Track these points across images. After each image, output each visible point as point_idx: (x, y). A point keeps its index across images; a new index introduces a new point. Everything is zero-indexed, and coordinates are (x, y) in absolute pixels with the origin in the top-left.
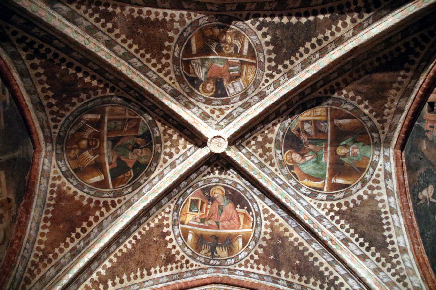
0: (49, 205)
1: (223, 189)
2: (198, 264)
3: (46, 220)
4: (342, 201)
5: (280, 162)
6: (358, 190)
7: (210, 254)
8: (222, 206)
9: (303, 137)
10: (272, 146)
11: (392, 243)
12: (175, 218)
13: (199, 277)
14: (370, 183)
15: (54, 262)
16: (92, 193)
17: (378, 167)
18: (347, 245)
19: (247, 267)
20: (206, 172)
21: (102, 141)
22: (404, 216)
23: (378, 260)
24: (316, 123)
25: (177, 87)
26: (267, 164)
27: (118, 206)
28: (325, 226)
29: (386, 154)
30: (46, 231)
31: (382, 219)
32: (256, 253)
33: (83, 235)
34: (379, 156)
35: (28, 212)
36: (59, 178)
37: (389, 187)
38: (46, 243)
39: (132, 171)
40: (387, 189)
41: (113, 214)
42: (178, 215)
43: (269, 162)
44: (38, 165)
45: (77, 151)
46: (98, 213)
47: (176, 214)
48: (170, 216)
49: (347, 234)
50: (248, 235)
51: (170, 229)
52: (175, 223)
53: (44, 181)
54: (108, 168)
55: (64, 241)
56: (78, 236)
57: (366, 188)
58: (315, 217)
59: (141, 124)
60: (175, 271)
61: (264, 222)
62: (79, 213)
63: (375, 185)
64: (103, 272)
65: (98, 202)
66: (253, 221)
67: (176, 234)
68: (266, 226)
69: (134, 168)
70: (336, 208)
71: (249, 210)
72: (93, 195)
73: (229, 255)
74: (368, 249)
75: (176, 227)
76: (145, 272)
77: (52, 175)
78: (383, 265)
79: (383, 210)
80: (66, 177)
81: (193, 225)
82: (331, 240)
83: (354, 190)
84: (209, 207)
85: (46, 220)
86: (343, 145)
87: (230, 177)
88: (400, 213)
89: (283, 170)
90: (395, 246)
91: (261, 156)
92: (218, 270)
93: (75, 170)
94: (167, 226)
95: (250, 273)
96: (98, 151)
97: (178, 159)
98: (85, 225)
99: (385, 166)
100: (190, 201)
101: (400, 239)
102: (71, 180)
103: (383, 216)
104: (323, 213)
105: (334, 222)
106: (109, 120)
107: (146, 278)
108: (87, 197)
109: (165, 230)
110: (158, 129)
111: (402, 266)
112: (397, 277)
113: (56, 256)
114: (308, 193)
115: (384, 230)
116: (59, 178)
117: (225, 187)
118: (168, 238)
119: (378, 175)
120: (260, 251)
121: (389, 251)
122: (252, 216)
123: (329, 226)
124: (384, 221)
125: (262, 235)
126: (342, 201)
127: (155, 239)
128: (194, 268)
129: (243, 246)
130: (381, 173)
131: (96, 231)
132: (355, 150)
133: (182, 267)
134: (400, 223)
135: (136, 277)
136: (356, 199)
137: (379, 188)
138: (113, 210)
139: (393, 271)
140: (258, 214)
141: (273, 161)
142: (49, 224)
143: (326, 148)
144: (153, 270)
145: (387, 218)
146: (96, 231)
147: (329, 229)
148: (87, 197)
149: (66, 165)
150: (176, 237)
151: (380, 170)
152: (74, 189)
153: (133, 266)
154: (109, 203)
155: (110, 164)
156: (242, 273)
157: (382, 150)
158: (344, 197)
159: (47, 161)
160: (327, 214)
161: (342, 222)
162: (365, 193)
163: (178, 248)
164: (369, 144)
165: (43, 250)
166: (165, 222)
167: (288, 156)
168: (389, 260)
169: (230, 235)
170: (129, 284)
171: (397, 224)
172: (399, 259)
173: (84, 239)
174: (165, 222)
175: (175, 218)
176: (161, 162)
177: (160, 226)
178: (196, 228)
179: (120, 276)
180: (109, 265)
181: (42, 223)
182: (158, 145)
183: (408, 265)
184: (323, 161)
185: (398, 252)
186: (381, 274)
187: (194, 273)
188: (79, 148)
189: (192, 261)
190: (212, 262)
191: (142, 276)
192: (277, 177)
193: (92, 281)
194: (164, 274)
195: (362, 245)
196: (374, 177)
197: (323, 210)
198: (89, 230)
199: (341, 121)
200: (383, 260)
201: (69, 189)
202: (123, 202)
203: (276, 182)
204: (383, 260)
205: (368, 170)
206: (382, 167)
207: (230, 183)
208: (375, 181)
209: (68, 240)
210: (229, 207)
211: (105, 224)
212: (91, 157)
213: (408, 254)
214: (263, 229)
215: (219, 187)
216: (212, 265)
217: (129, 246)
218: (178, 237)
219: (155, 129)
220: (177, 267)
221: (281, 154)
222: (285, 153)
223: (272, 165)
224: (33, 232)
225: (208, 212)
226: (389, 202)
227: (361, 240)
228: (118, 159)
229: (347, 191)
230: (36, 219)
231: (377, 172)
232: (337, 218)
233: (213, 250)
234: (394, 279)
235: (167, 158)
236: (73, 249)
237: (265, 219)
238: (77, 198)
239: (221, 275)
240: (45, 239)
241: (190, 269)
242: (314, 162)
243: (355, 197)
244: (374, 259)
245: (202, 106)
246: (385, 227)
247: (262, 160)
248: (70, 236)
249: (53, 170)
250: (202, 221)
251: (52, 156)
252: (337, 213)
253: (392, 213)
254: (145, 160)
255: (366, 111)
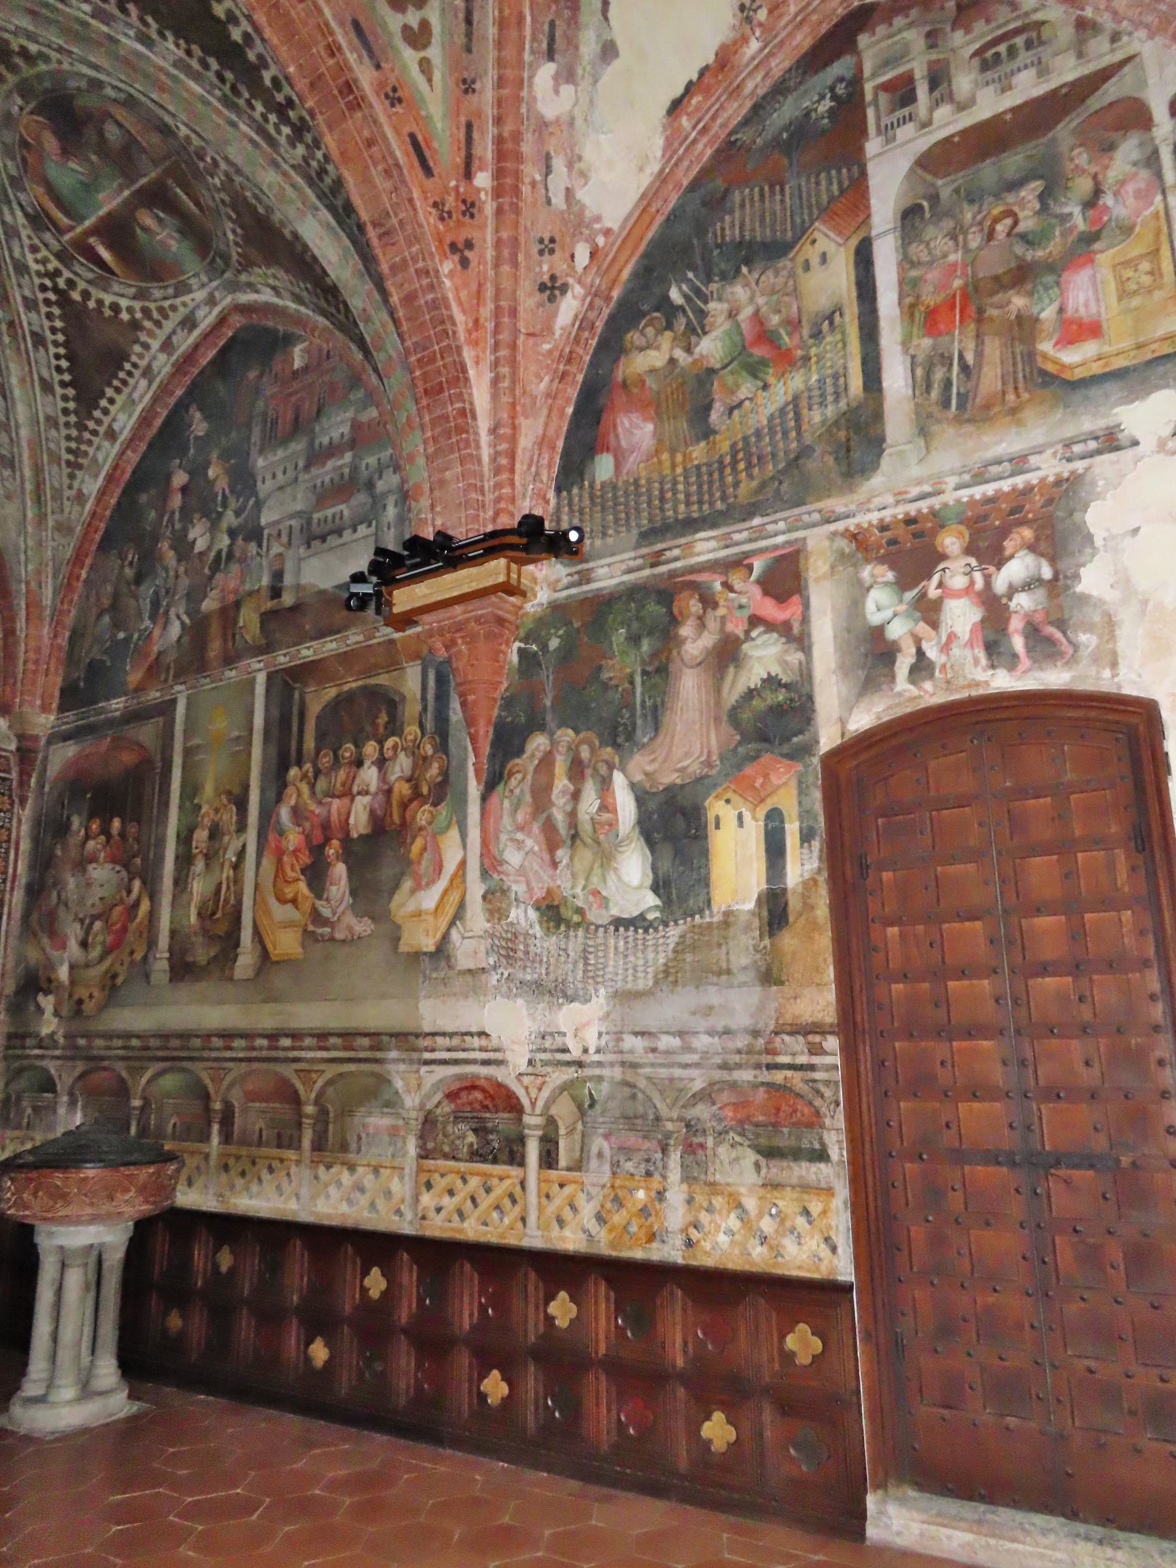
4: (82, 285)
6: (122, 296)
9: (90, 133)
11: (106, 412)
14: (152, 306)
17: (186, 298)
18: (35, 346)
22: (156, 399)
23: (66, 411)
24: (130, 143)
28: (20, 286)
29: (217, 294)
31: (122, 368)
34: (203, 286)
37: (175, 339)
40: (169, 338)
49: (48, 333)
57: (137, 305)
58: (12, 258)
63: (156, 315)
70: (61, 282)
74: (63, 384)
78: (67, 425)
79: (134, 358)
82: (11, 324)
83: (116, 288)
86: (158, 217)
88: (155, 386)
90: (107, 420)
99: (198, 306)
101: (122, 417)
103: (127, 366)
104: (34, 267)
105: (41, 296)
111: (91, 451)
112: (71, 457)
114: (29, 210)
115: (110, 385)
119: (174, 308)
121: (90, 417)
123: (27, 293)
124: (122, 375)
126: (82, 285)
130: (182, 312)
132: (173, 242)
134: (142, 397)
136: (107, 303)
137: (158, 324)
139: (73, 445)
143: (121, 189)
145: (130, 374)
147: (24, 298)
151: (184, 305)
157: (215, 284)
158: (89, 282)
160: (38, 274)
161: (56, 311)
162: (130, 310)
164: (204, 258)
168: (81, 427)
171: (136, 396)
172: (96, 440)
183: (100, 457)
184: (101, 196)
185: (102, 430)
186: (53, 433)
195: (59, 369)
196: (166, 304)
197: (37, 261)
199: (178, 190)
200: (73, 419)
204: (73, 419)
205: (166, 287)
206: (191, 305)
208: (161, 310)
213: (113, 444)
221: (21, 109)
222: (32, 113)
226: (154, 358)
227: (64, 364)
229: (101, 277)
231: (178, 301)
232: (52, 297)
234: (66, 456)
242: (81, 183)
243: (108, 299)
244: (61, 404)
246: (116, 383)
252: (56, 289)
253: (144, 375)
255: (231, 237)
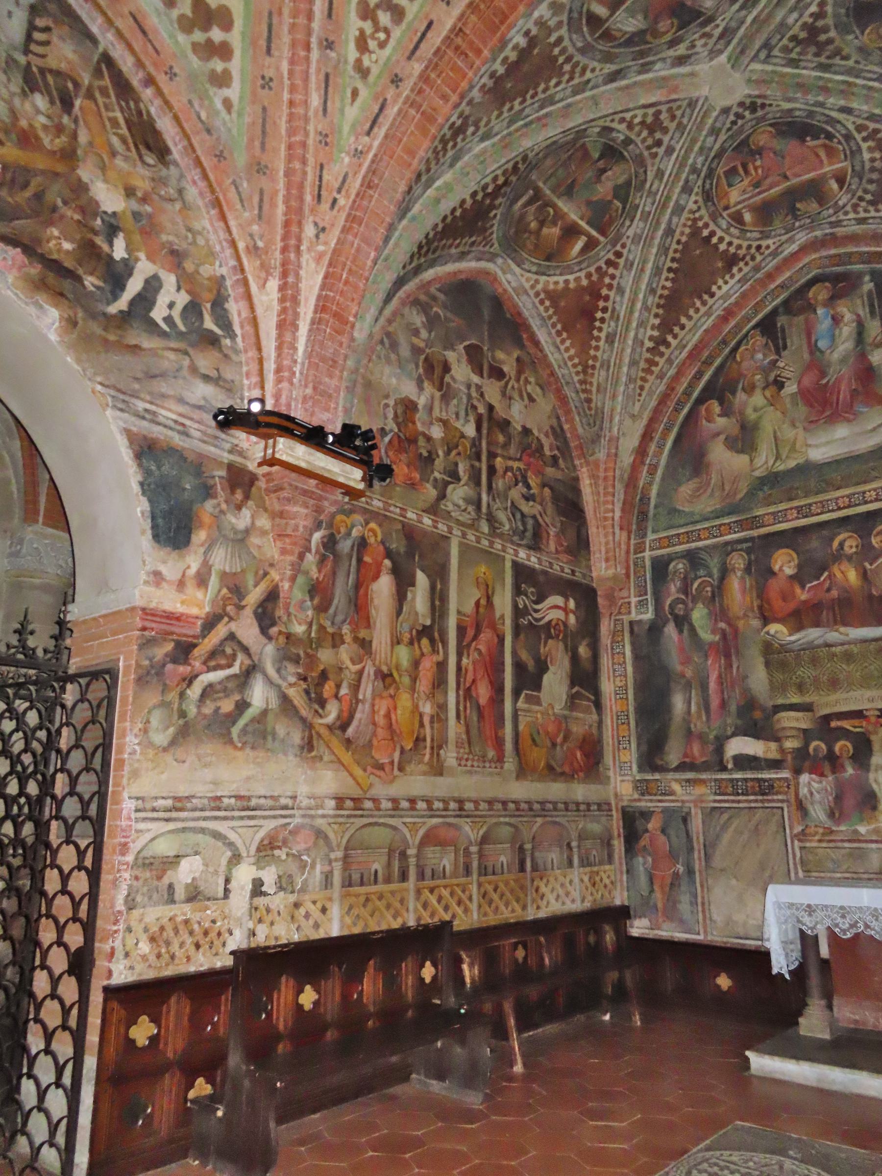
0: (550, 317)
1: (770, 129)
2: (775, 240)
3: (559, 333)
5: (861, 50)
7: (790, 217)
8: (781, 150)
10: (832, 34)
12: (712, 209)
13: (786, 253)
15: (598, 365)
16: (583, 266)
19: (857, 213)
20: (728, 125)
21: (554, 206)
25: (610, 68)
26: (837, 60)
27: (625, 252)
30: (568, 343)
32: (866, 191)
33: (607, 316)
35: (537, 344)
36: (537, 281)
38: (577, 355)
39: (615, 201)
41: (625, 266)
42: (714, 204)
43: (838, 58)
44: (505, 290)
45: (532, 238)
46: (607, 280)
47: (710, 204)
48: (703, 212)
50: (843, 172)
51: (712, 226)
52: (714, 217)
53: (524, 298)
54: (583, 224)
55: (592, 337)
56: (602, 320)
59: (589, 146)
60: (746, 269)
61: (864, 146)
62: (587, 298)
64: (656, 333)
65: (599, 269)
66: (844, 150)
67: (724, 227)
68: (870, 149)
69: (616, 196)
71: (829, 136)
72: (588, 266)
73: (821, 205)
75: (720, 219)
76: (706, 297)
77: (527, 286)
80: (544, 274)
81: (744, 201)
84: (758, 163)
85: (559, 333)
87: (774, 109)
89: (871, 58)
91: (817, 55)
92: (812, 229)
93: (548, 258)
94: (706, 225)
95: (865, 219)
96: (559, 215)
97: (672, 138)
98: (601, 304)
100: (722, 175)
102: (552, 272)
106: (544, 183)
107: (710, 301)
108: (582, 274)
109: (705, 233)
110: (619, 132)
113: (595, 358)
116: (537, 281)
117: (771, 125)
118: (715, 240)
120: (872, 187)
122: (839, 143)
125: (868, 166)
127: (698, 252)
128: (773, 247)
129: (841, 188)
131: (618, 299)
133: (753, 258)
135: (697, 310)
138: (621, 261)
140: (848, 137)
141: (844, 53)
142: (565, 335)
144: (714, 288)
146: (618, 299)
148: (582, 274)
149: (532, 263)
150: (727, 231)
152: (561, 279)
153: (687, 301)
154: (613, 258)
155: (582, 219)
156: (853, 222)
159: (509, 276)
163: (736, 242)
165: (579, 364)
166: (700, 224)
167: (874, 36)
169: (812, 181)
170: (692, 323)
173: (612, 317)
174: (700, 224)
175: (712, 209)
176: (649, 162)
177: (695, 232)
178: (752, 201)
179: (677, 323)
180: (657, 321)
181: (558, 340)
182: (631, 147)
187: (775, 254)
188: (530, 232)
189: (764, 243)
190: (797, 224)
191: (704, 303)
192: (862, 71)
193: (648, 350)
194: (732, 282)
198: (609, 304)
201: (556, 283)
202: (629, 242)
203: (865, 78)
207: (778, 115)
209: (595, 333)
210: (791, 146)
211: (623, 284)
212: (554, 230)
214: (866, 156)
215: (761, 130)
216: (801, 227)
217: (669, 284)
218: (728, 229)
219: (614, 134)
220: (746, 264)
221: (857, 38)
222: (863, 33)
223: (846, 58)
224: (557, 355)
225: (760, 171)
228: (589, 203)
230: (548, 340)
233: (793, 211)
235: (654, 150)
236: (607, 337)
237: (865, 139)
238: (572, 285)
239: (818, 233)
240: (572, 352)
241: (767, 252)
245: (671, 53)
247: (822, 59)
248: (594, 328)
249: (523, 280)
250: (757, 185)
251: (509, 266)
254: (625, 176)
